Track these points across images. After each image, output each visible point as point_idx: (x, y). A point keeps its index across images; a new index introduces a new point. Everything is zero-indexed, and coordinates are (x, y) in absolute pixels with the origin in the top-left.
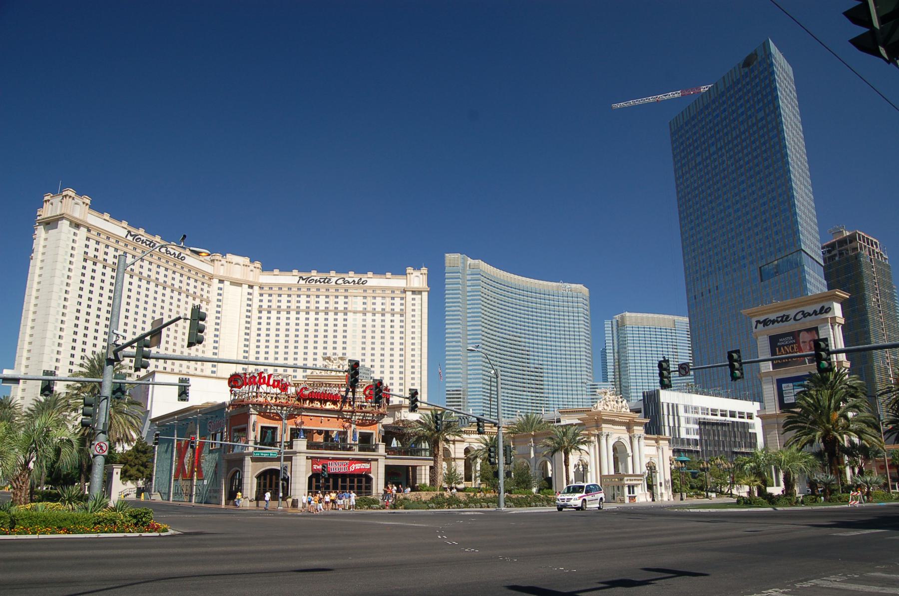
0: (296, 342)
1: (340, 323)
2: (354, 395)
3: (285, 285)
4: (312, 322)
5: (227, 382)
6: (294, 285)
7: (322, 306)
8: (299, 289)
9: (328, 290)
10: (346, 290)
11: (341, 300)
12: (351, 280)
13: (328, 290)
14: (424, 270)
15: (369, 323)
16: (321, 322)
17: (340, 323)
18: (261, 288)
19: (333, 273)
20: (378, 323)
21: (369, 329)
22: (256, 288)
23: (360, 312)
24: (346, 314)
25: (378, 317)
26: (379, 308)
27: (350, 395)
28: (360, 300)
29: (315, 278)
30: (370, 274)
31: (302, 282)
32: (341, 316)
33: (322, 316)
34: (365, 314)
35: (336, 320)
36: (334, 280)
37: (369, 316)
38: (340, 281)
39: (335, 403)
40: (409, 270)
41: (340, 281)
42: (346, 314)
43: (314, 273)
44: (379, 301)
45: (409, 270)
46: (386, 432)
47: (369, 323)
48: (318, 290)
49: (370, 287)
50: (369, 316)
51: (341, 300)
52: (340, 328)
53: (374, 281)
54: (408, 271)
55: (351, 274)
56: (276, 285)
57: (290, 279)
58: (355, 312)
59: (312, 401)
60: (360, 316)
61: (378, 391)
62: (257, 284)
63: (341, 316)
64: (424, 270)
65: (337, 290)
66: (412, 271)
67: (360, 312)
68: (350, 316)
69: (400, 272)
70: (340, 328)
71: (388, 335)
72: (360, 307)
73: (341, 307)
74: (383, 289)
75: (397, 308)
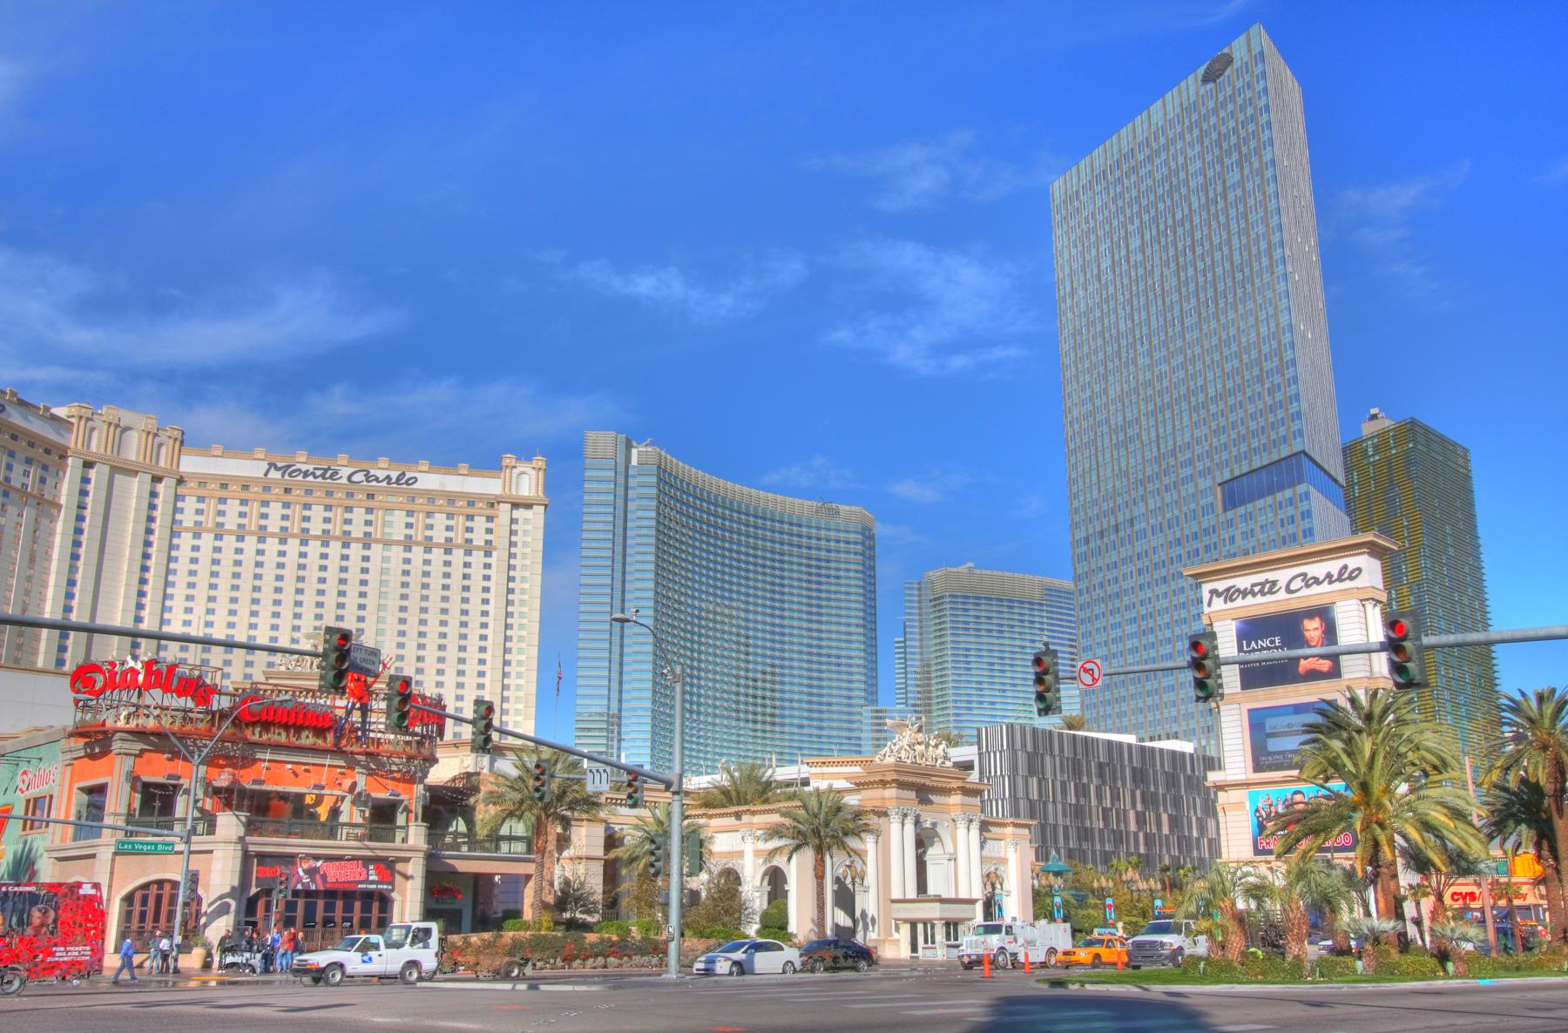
0: (255, 601)
1: (355, 564)
2: (364, 715)
3: (235, 479)
4: (249, 556)
5: (68, 680)
7: (316, 528)
8: (267, 489)
9: (329, 494)
10: (371, 496)
11: (359, 515)
12: (381, 474)
13: (329, 494)
14: (539, 461)
15: (417, 566)
16: (313, 560)
17: (355, 564)
19: (343, 459)
20: (437, 568)
21: (415, 580)
23: (398, 543)
24: (367, 546)
25: (437, 555)
26: (439, 536)
27: (356, 717)
28: (399, 518)
29: (304, 468)
30: (424, 465)
31: (274, 474)
32: (356, 550)
33: (314, 548)
34: (408, 549)
35: (447, 564)
37: (417, 554)
39: (320, 732)
40: (509, 459)
41: (359, 477)
42: (367, 546)
43: (301, 456)
44: (440, 520)
45: (509, 459)
46: (432, 797)
47: (417, 566)
48: (309, 492)
49: (423, 492)
50: (417, 554)
51: (359, 515)
52: (354, 575)
53: (429, 481)
54: (506, 462)
55: (384, 462)
56: (214, 477)
57: (251, 468)
58: (388, 543)
59: (266, 726)
60: (397, 553)
61: (416, 713)
63: (356, 550)
64: (539, 461)
65: (350, 495)
67: (398, 543)
68: (376, 551)
69: (488, 463)
70: (354, 575)
71: (455, 595)
72: (399, 533)
73: (357, 530)
74: (451, 498)
75: (479, 538)
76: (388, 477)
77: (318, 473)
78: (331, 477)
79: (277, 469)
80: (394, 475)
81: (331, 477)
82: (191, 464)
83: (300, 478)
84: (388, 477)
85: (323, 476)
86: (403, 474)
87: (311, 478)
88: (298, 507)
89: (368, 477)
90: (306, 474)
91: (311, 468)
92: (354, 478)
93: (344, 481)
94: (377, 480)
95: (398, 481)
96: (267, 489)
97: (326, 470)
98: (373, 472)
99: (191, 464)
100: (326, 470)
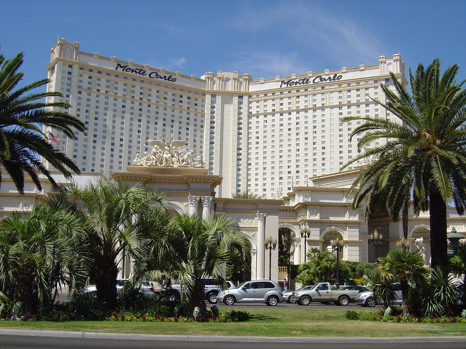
3: (270, 91)
6: (277, 90)
8: (282, 93)
9: (306, 90)
12: (327, 77)
18: (250, 97)
22: (245, 98)
31: (284, 86)
36: (311, 80)
38: (318, 80)
41: (318, 80)
48: (298, 91)
62: (246, 94)
66: (384, 60)
76: (330, 78)
77: (301, 82)
78: (306, 83)
79: (285, 83)
80: (332, 76)
81: (306, 83)
82: (253, 88)
83: (294, 85)
84: (330, 78)
85: (303, 83)
86: (336, 75)
87: (298, 85)
88: (295, 98)
89: (321, 79)
90: (296, 83)
91: (298, 80)
92: (315, 81)
93: (312, 83)
94: (325, 80)
95: (334, 79)
96: (282, 93)
97: (304, 80)
98: (323, 77)
99: (253, 88)
100: (304, 80)
